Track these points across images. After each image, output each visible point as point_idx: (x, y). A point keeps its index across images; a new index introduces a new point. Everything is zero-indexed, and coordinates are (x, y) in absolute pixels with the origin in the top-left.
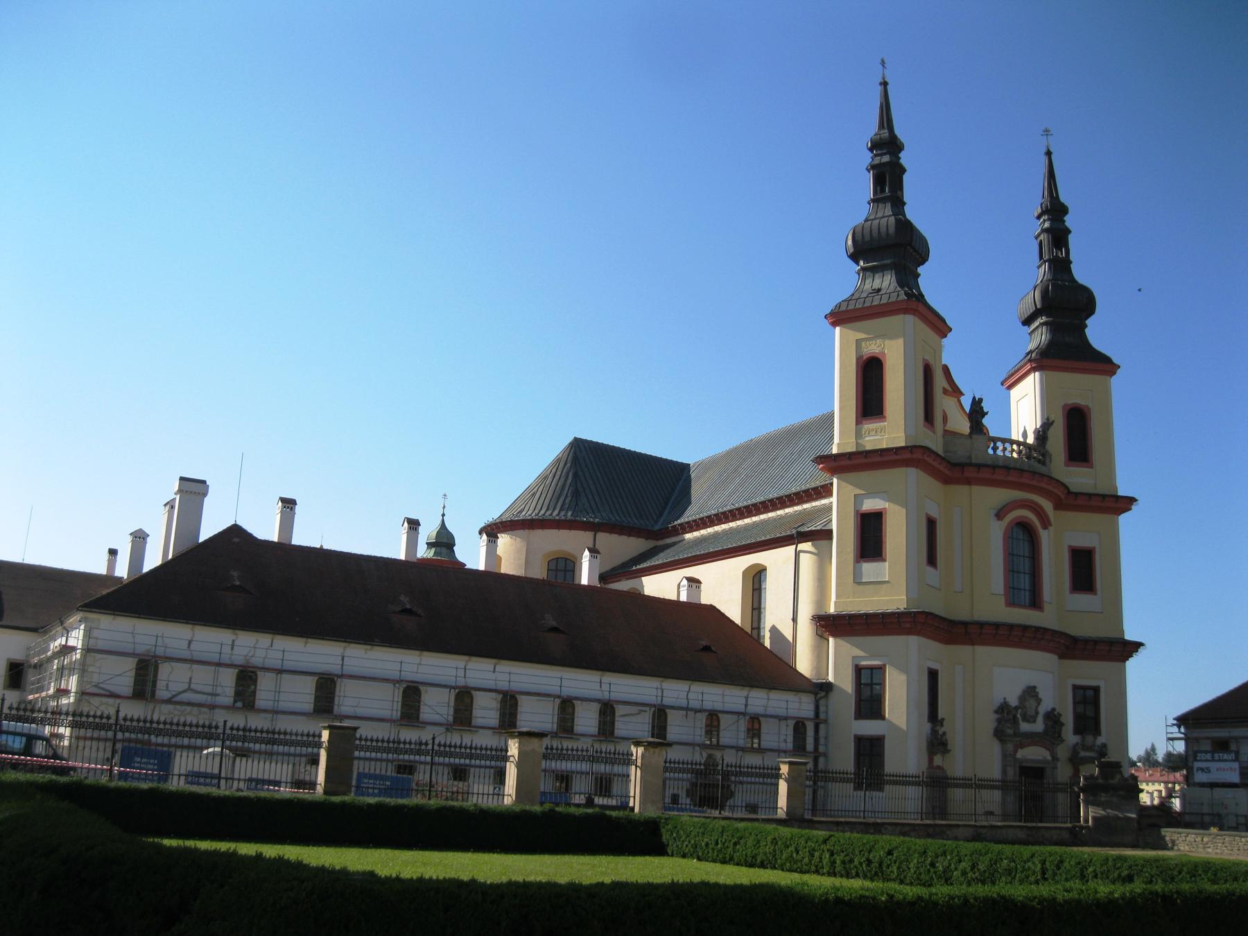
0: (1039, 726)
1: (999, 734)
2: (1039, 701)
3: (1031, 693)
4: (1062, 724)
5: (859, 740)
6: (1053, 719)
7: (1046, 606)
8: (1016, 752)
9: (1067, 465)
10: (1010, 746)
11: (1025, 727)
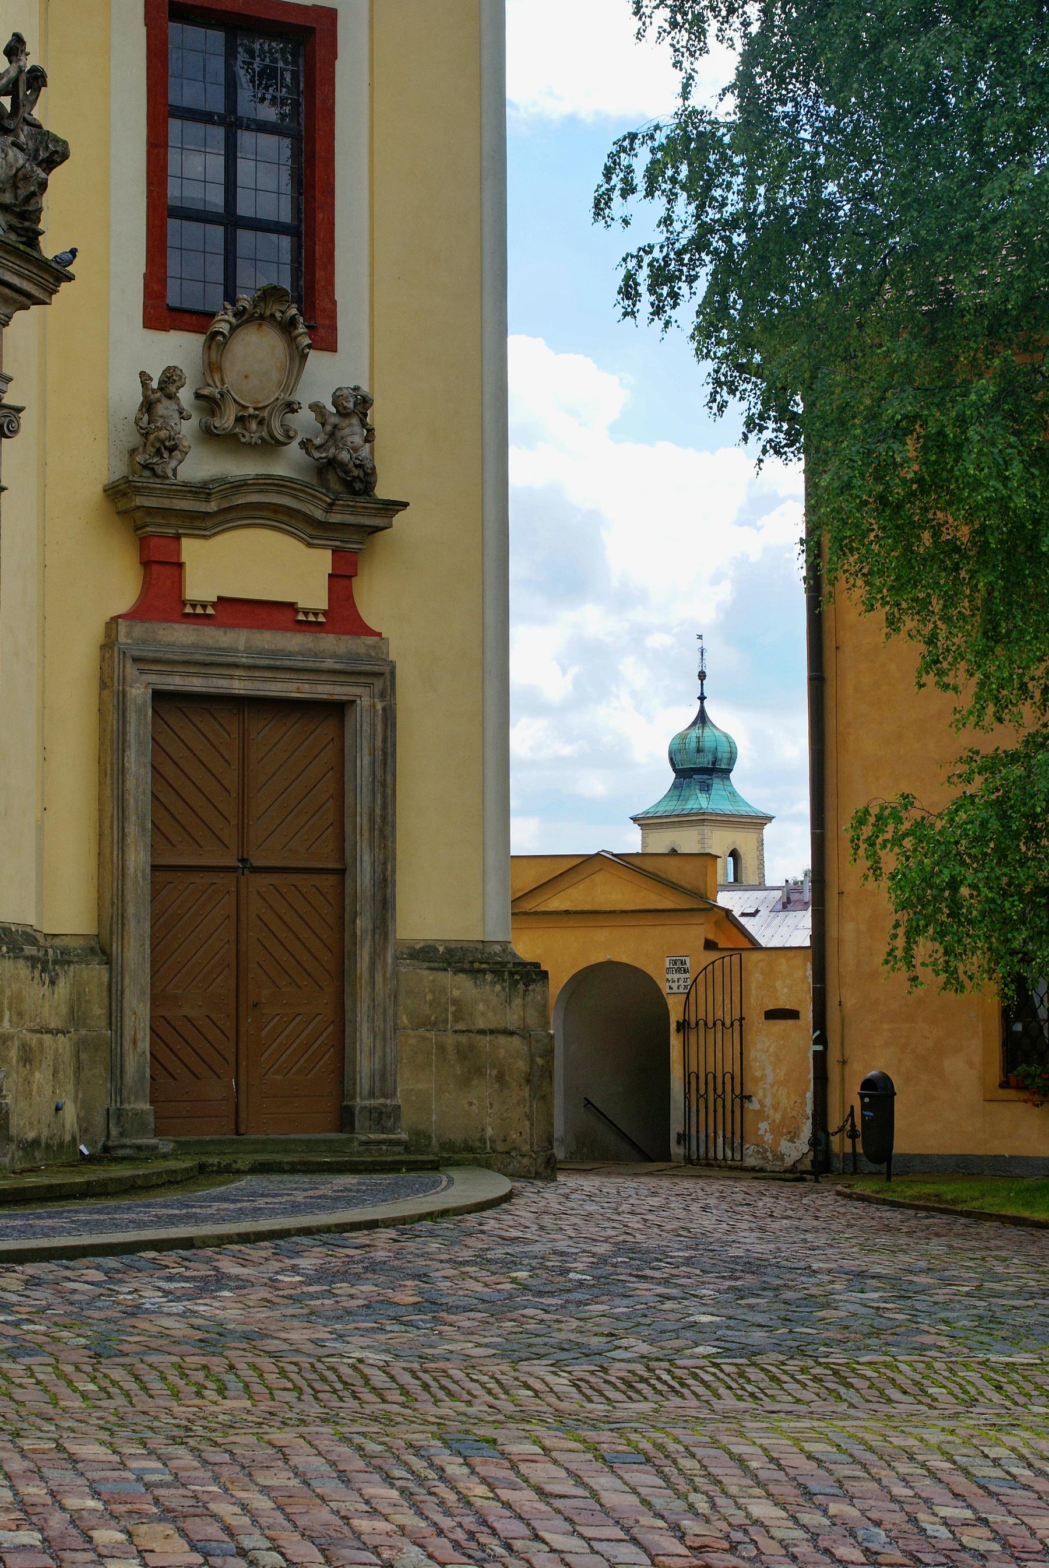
4: (52, 154)
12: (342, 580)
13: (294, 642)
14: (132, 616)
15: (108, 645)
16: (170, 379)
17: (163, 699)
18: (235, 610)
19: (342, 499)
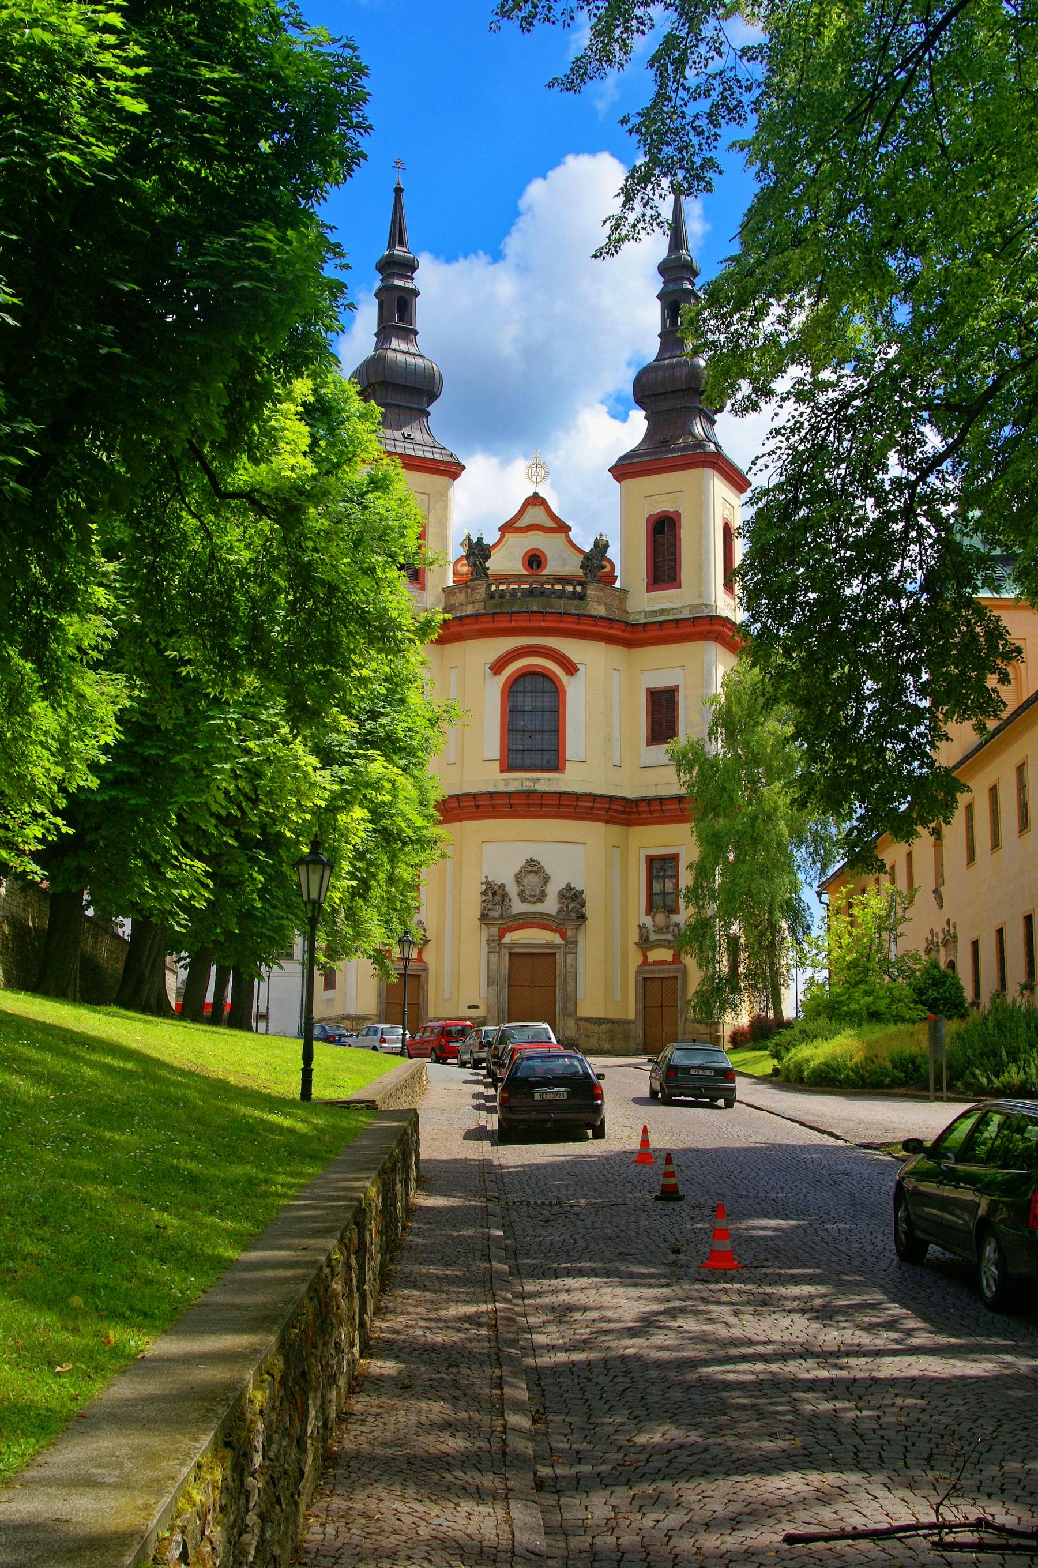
0: (551, 905)
1: (484, 917)
3: (533, 867)
6: (572, 897)
8: (501, 936)
10: (495, 931)
11: (518, 907)
17: (645, 979)
18: (656, 963)
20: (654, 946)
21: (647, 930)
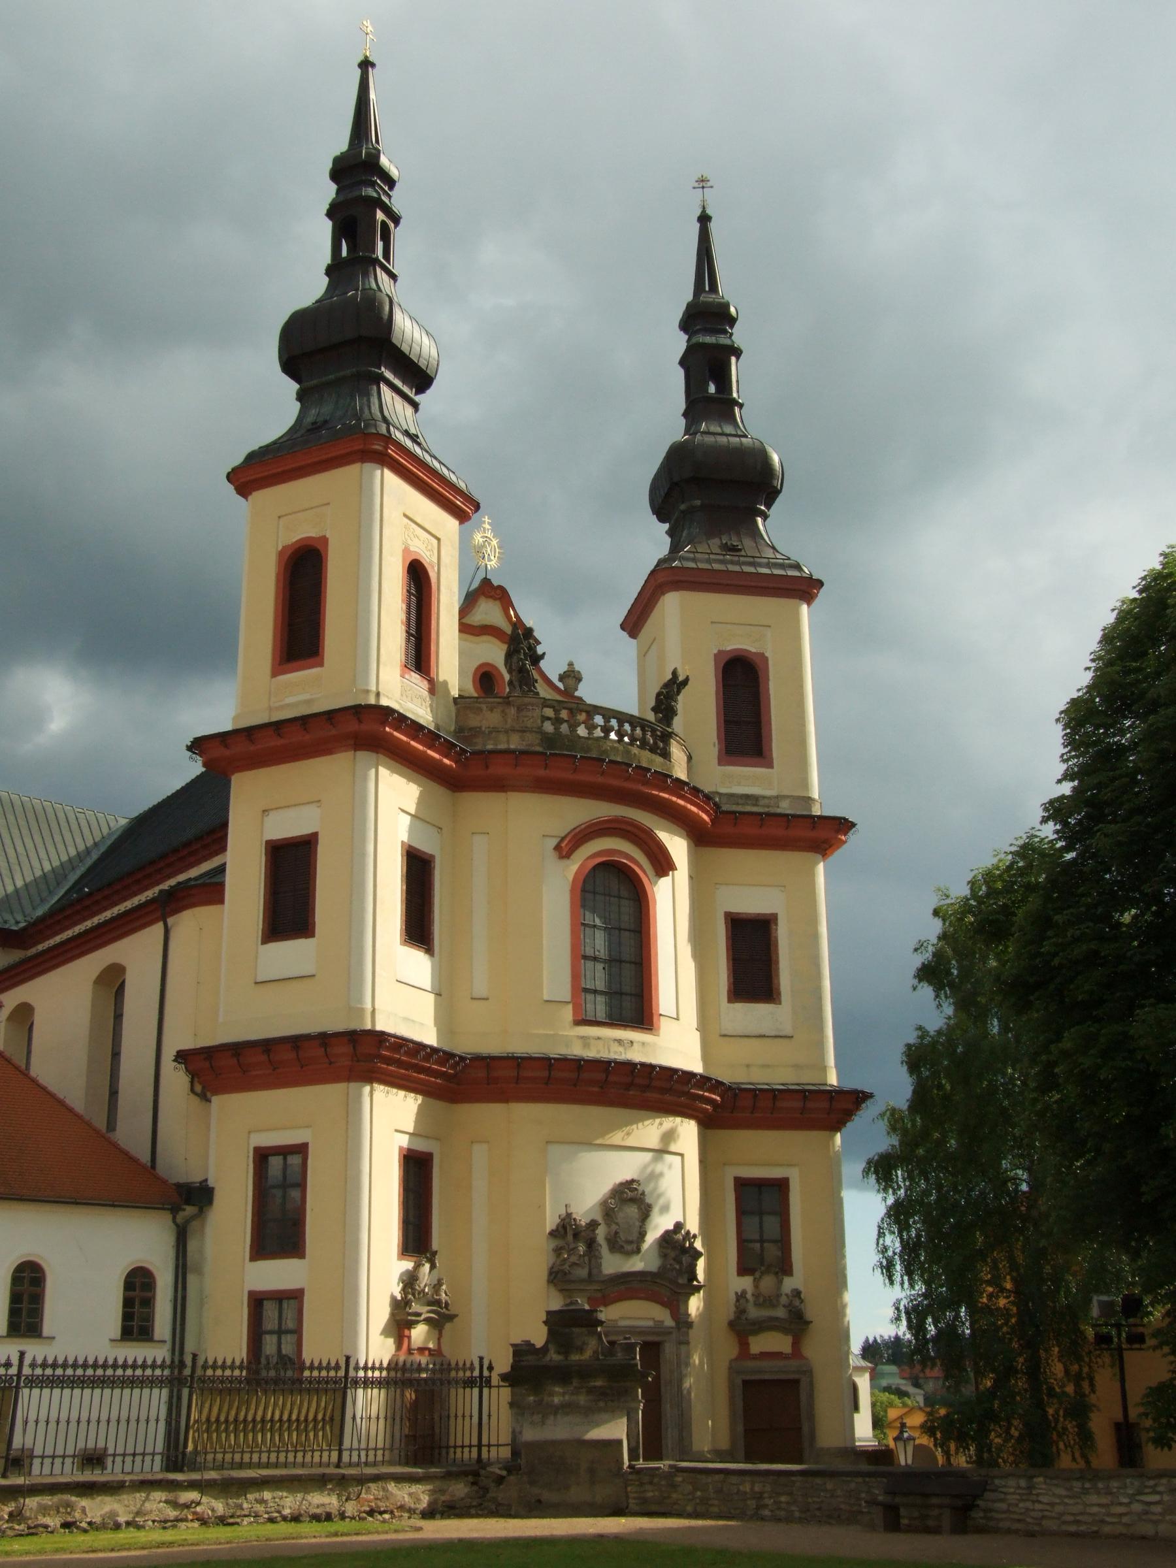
2: (646, 1212)
5: (257, 1301)
6: (675, 1245)
7: (664, 1025)
9: (720, 764)
12: (796, 1344)
13: (781, 1363)
14: (736, 1359)
15: (730, 1368)
16: (744, 1292)
17: (745, 1382)
19: (796, 1322)
20: (760, 1326)
21: (747, 1301)
